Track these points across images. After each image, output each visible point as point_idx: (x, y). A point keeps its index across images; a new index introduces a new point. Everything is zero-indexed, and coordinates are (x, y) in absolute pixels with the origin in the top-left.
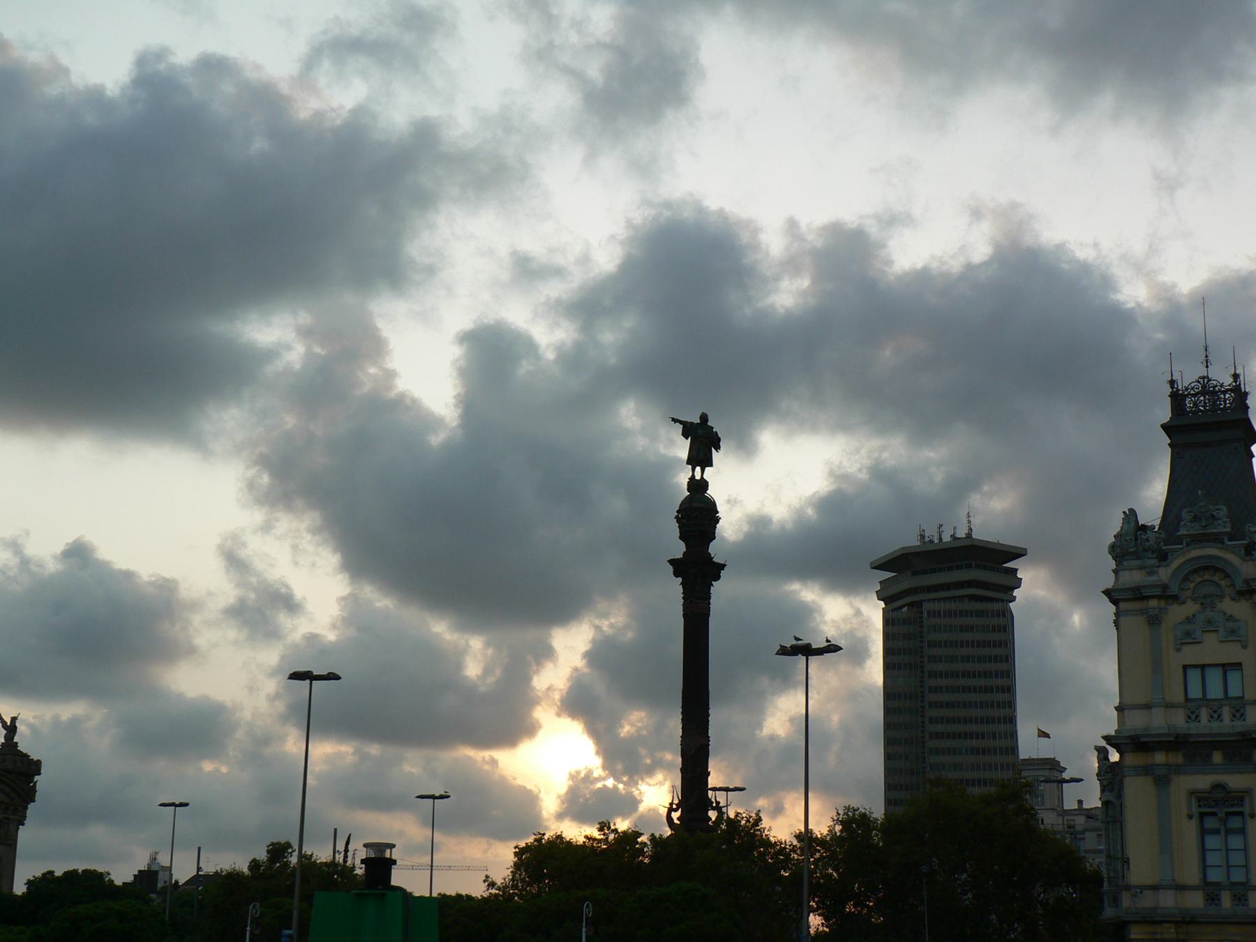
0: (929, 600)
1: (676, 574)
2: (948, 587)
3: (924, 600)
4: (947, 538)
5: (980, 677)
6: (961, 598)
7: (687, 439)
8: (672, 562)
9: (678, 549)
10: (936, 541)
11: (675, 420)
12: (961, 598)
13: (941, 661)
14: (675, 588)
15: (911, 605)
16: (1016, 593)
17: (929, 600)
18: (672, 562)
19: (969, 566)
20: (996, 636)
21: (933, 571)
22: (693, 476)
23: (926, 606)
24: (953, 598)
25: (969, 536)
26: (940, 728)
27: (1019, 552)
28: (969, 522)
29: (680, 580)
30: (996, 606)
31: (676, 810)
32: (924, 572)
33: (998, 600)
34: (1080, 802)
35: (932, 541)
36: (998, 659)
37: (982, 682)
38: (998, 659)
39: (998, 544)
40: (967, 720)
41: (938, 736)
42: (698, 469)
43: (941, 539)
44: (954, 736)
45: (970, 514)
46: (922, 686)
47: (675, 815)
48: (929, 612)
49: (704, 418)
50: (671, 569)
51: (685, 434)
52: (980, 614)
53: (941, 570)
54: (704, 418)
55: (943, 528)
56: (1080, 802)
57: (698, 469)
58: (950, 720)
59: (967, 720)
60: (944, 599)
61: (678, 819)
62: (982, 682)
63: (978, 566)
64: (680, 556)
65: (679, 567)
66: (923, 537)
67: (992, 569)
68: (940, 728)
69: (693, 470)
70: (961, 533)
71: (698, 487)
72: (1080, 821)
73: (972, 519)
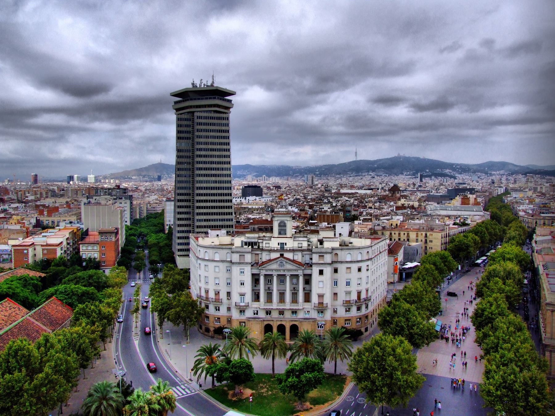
0: (198, 111)
2: (205, 106)
10: (198, 86)
12: (211, 111)
13: (202, 138)
15: (188, 112)
16: (231, 110)
17: (198, 111)
19: (215, 98)
20: (224, 128)
21: (199, 99)
23: (196, 114)
24: (207, 111)
25: (212, 85)
26: (201, 166)
28: (213, 79)
30: (224, 115)
32: (195, 99)
33: (226, 113)
35: (196, 87)
36: (224, 137)
37: (219, 147)
38: (224, 137)
40: (212, 163)
46: (193, 147)
48: (197, 117)
53: (202, 99)
58: (205, 163)
60: (204, 111)
63: (218, 98)
66: (193, 84)
67: (221, 99)
68: (201, 166)
70: (209, 84)
73: (214, 78)
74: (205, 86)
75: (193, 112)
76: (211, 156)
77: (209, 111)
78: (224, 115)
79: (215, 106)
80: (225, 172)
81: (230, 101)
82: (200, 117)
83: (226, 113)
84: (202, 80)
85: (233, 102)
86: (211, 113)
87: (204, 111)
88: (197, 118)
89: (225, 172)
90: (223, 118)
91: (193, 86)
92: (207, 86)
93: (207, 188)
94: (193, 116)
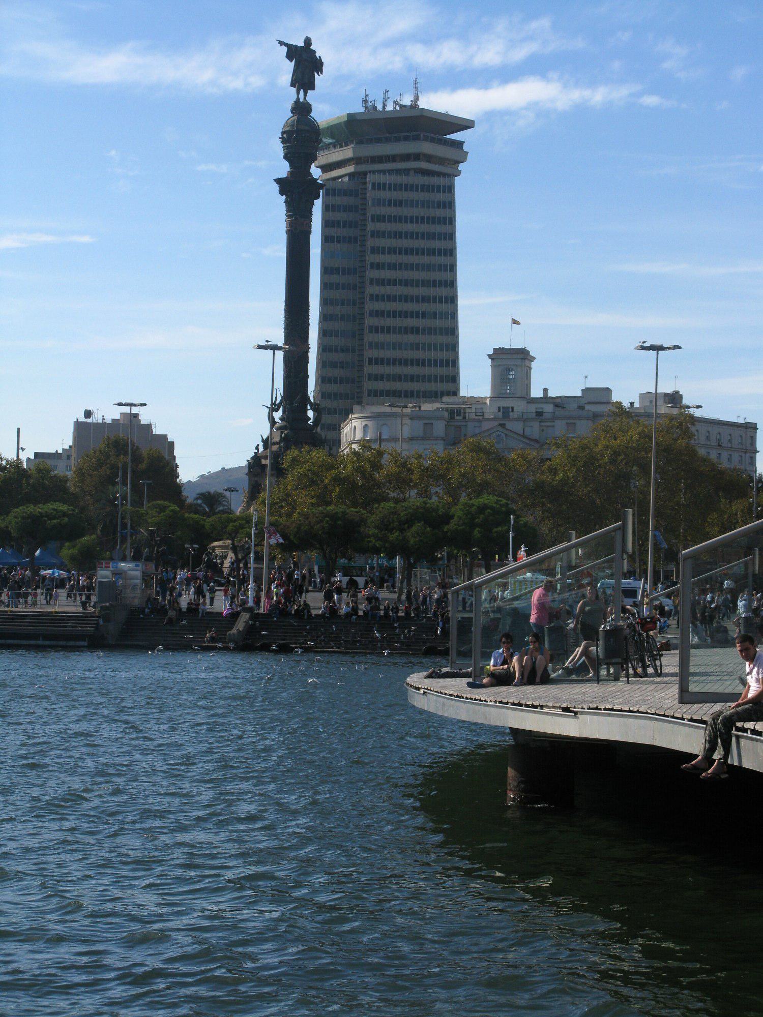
0: (374, 172)
1: (282, 192)
2: (393, 158)
3: (370, 172)
4: (390, 108)
5: (423, 254)
6: (407, 171)
7: (291, 61)
8: (279, 181)
9: (283, 169)
10: (380, 108)
11: (281, 43)
12: (407, 171)
14: (279, 203)
16: (461, 167)
17: (374, 172)
18: (279, 181)
22: (298, 99)
23: (370, 178)
27: (463, 123)
29: (284, 197)
30: (441, 181)
31: (277, 410)
33: (444, 175)
34: (546, 390)
35: (375, 108)
39: (447, 115)
40: (407, 299)
41: (379, 314)
42: (302, 92)
43: (384, 107)
44: (393, 314)
45: (418, 80)
47: (278, 415)
48: (373, 184)
49: (308, 41)
50: (276, 187)
51: (290, 56)
52: (426, 188)
54: (308, 41)
55: (389, 95)
56: (546, 390)
57: (302, 92)
58: (391, 298)
59: (407, 299)
60: (390, 172)
61: (281, 419)
62: (426, 259)
63: (426, 139)
64: (284, 175)
65: (284, 185)
66: (365, 101)
69: (298, 93)
71: (302, 109)
72: (548, 408)
74: (398, 108)
75: (364, 174)
76: (407, 283)
77: (404, 170)
78: (441, 181)
79: (417, 157)
80: (438, 323)
81: (459, 145)
82: (379, 184)
83: (444, 175)
84: (387, 91)
85: (465, 148)
86: (408, 174)
87: (390, 172)
88: (373, 188)
89: (438, 323)
90: (439, 187)
91: (366, 108)
92: (402, 107)
93: (394, 362)
94: (365, 183)
